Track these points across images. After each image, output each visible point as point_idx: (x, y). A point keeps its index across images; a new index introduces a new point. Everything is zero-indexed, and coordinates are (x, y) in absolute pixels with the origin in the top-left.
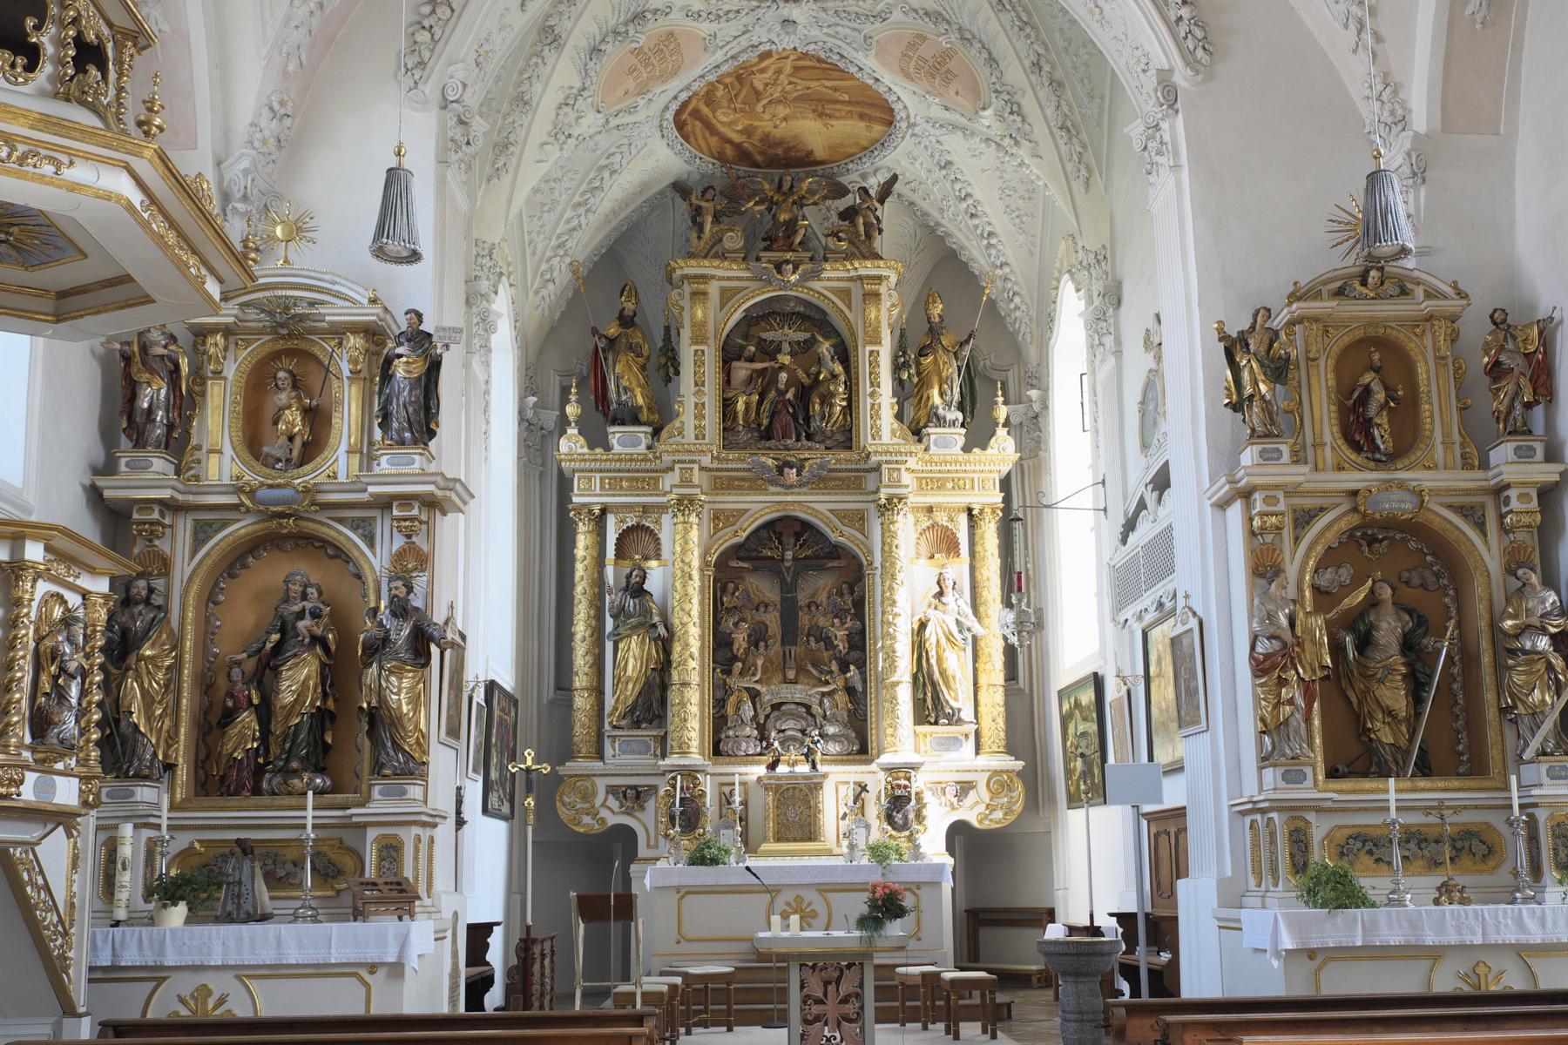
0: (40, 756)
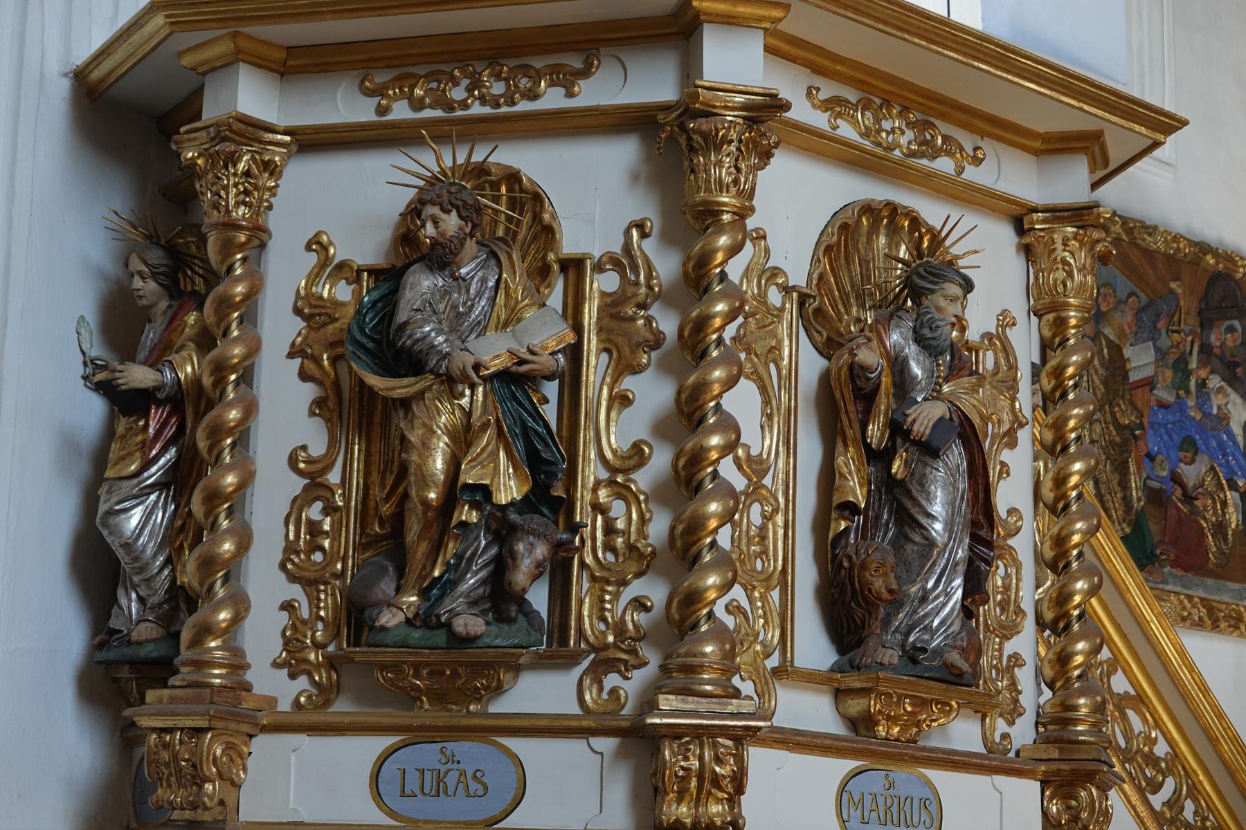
0: (855, 706)
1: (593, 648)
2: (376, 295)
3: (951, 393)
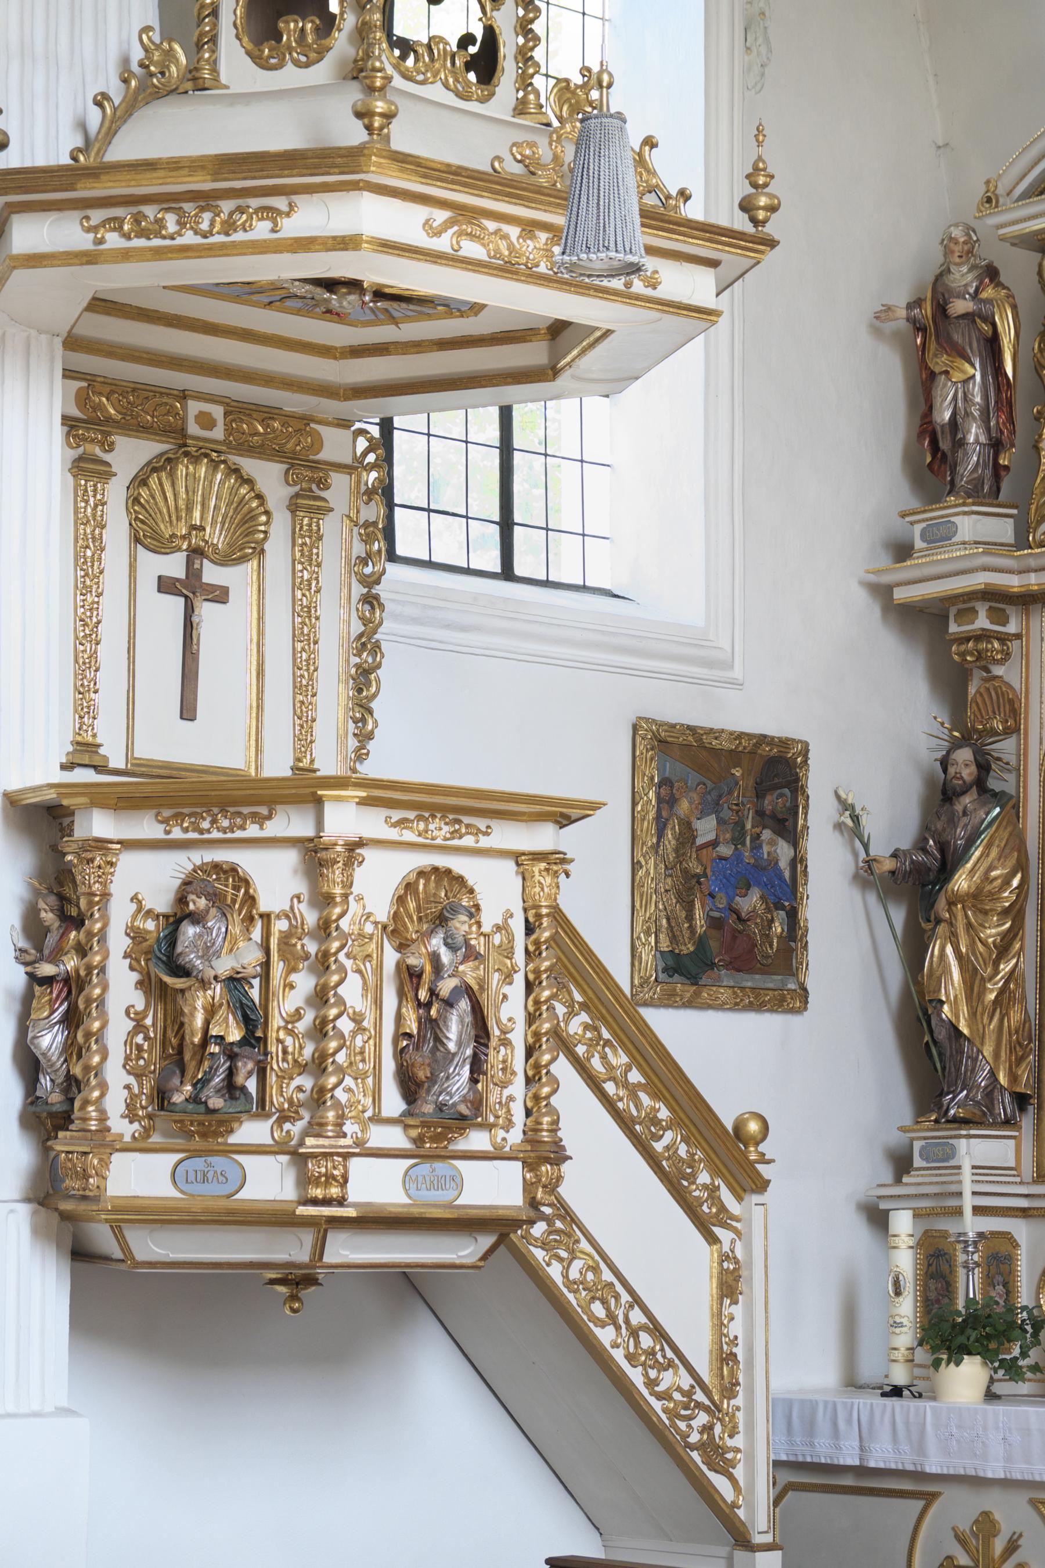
1: (278, 1110)
2: (166, 932)
3: (463, 972)
